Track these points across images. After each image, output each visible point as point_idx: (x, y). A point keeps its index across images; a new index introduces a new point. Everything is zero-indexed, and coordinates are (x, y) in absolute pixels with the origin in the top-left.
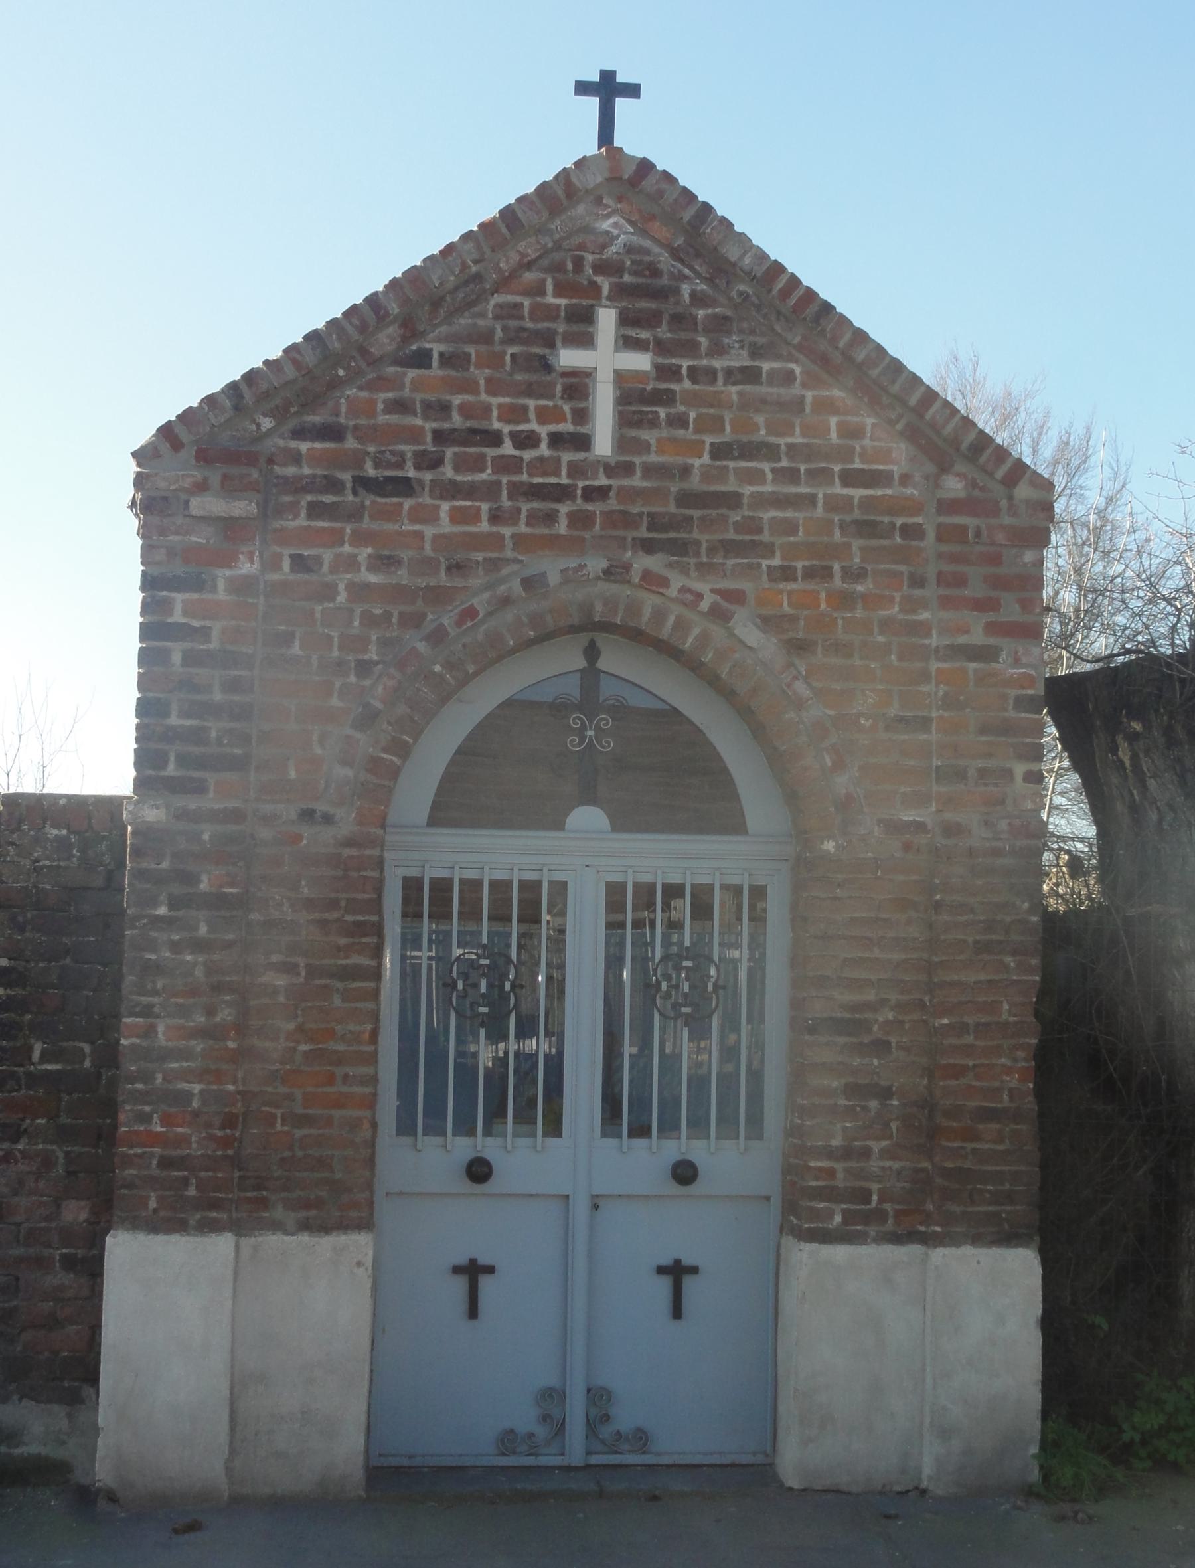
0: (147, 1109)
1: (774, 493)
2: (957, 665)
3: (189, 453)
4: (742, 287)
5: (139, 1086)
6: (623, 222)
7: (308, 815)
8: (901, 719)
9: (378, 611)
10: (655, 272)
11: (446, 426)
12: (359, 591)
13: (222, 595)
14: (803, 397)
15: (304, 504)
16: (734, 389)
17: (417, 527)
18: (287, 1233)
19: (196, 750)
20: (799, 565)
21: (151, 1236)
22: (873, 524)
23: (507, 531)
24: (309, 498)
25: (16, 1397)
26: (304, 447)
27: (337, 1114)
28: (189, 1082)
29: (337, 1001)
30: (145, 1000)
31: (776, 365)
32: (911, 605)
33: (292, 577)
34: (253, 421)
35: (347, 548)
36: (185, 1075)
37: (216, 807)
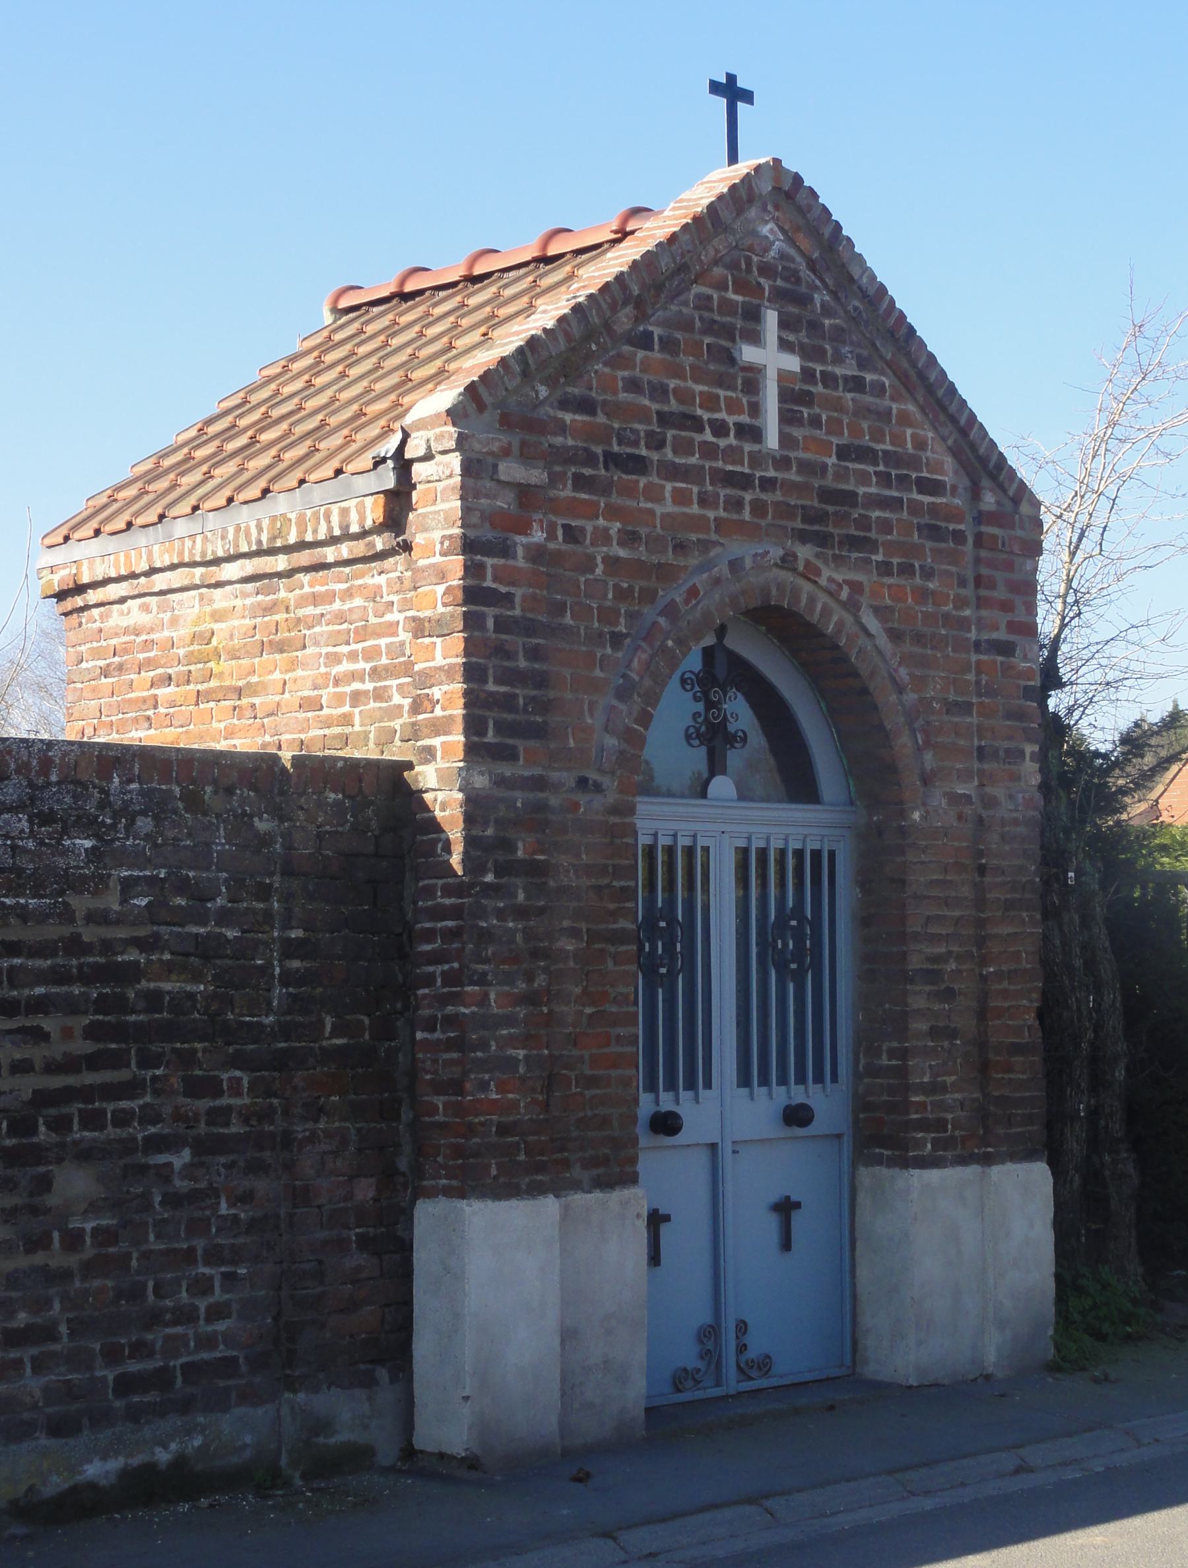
0: (487, 1076)
1: (878, 495)
2: (991, 657)
3: (491, 416)
4: (857, 303)
5: (479, 1054)
6: (776, 229)
7: (582, 782)
8: (956, 704)
9: (625, 585)
10: (798, 280)
11: (666, 409)
12: (612, 563)
13: (521, 562)
14: (891, 408)
15: (570, 474)
16: (849, 396)
17: (650, 505)
18: (584, 1191)
19: (510, 717)
20: (895, 561)
21: (497, 1203)
22: (935, 528)
23: (711, 514)
24: (573, 470)
25: (325, 1386)
26: (568, 417)
27: (614, 1073)
28: (515, 1048)
29: (610, 964)
30: (481, 967)
31: (875, 377)
32: (961, 603)
33: (565, 547)
34: (533, 388)
35: (601, 522)
36: (511, 1041)
37: (526, 773)
